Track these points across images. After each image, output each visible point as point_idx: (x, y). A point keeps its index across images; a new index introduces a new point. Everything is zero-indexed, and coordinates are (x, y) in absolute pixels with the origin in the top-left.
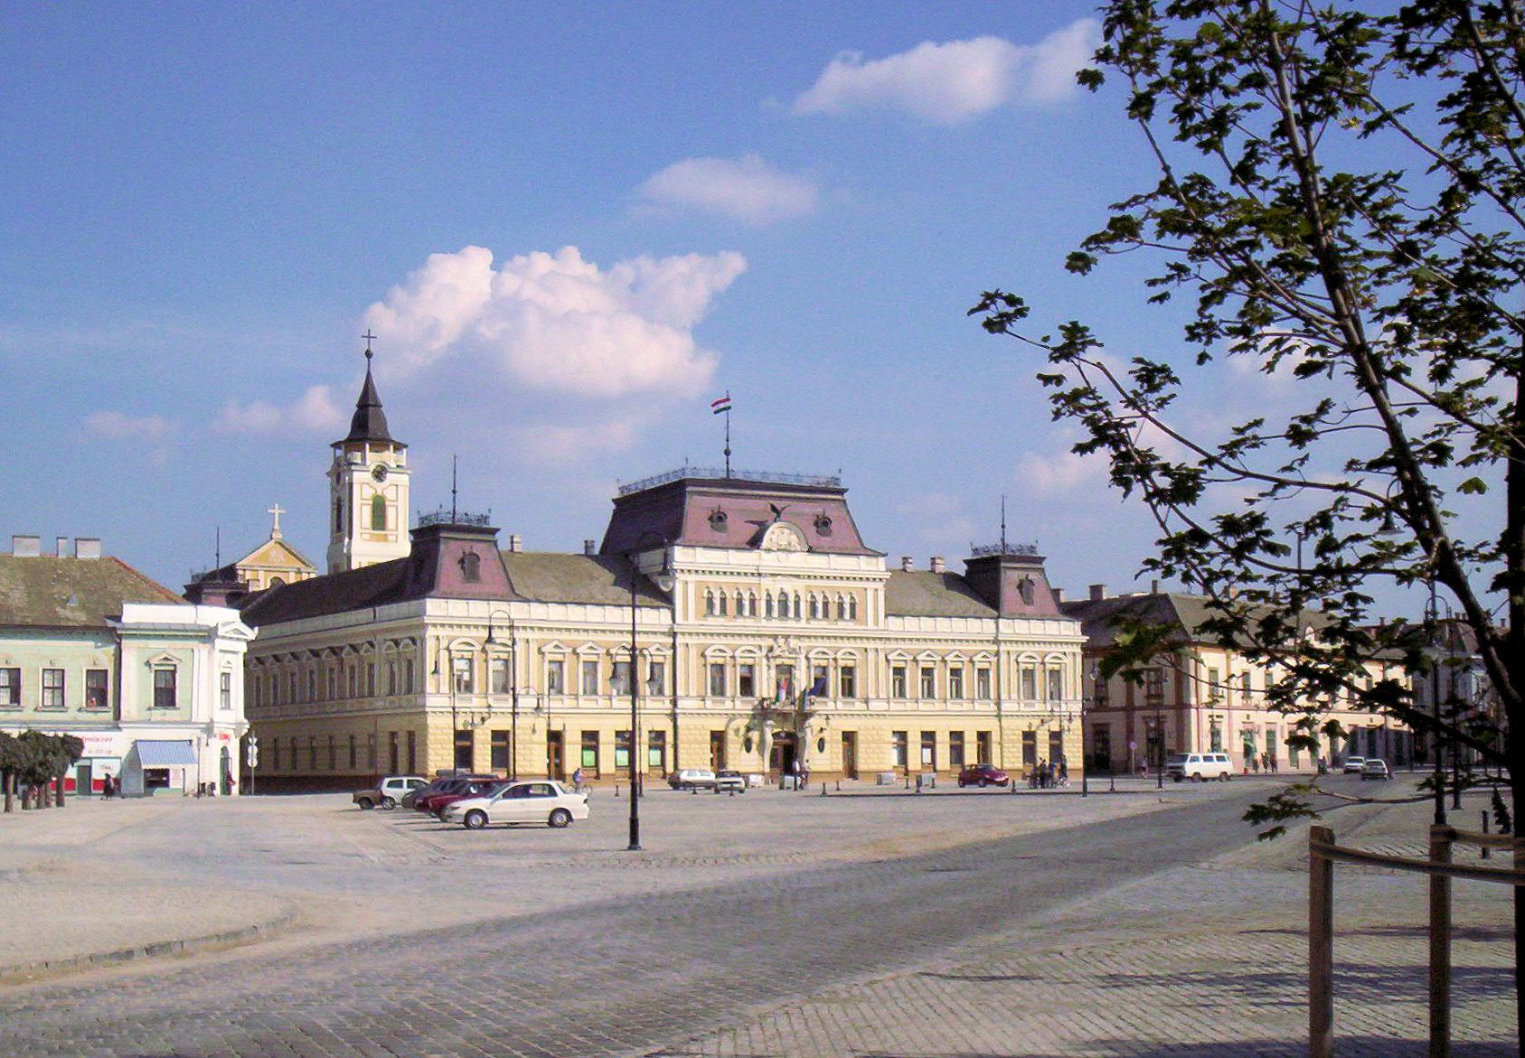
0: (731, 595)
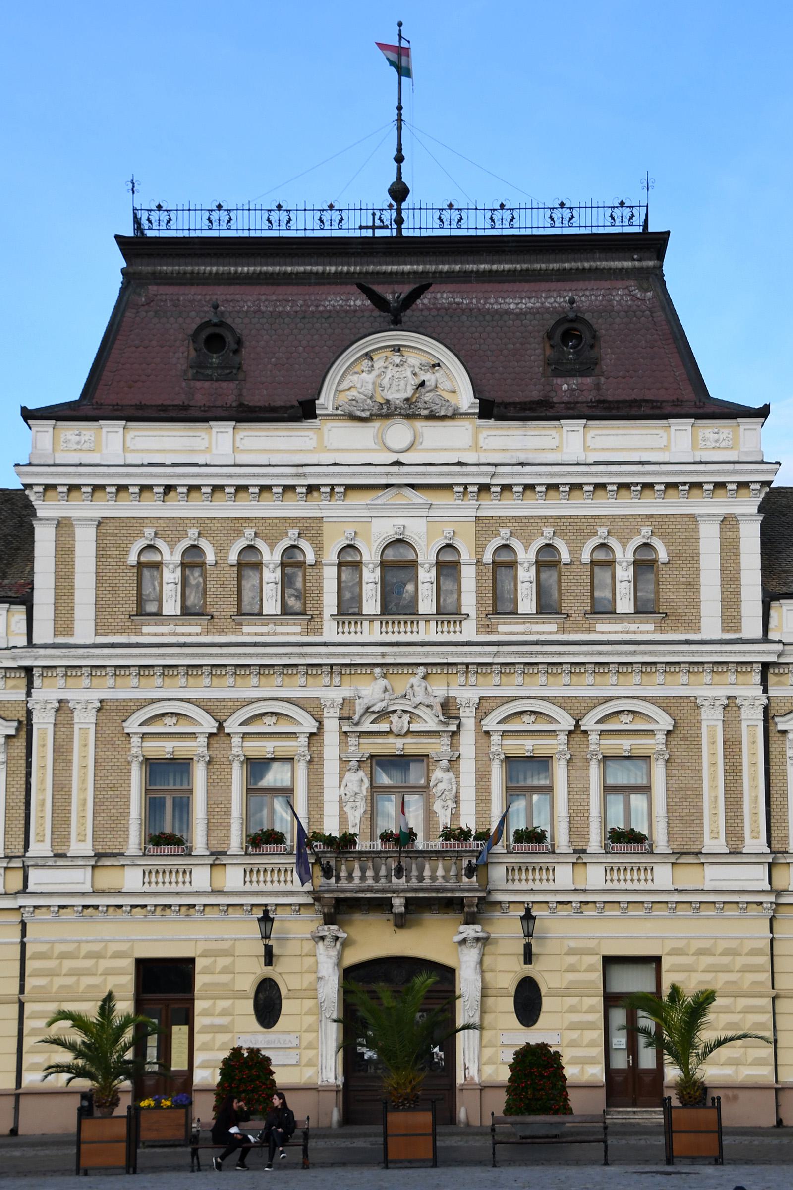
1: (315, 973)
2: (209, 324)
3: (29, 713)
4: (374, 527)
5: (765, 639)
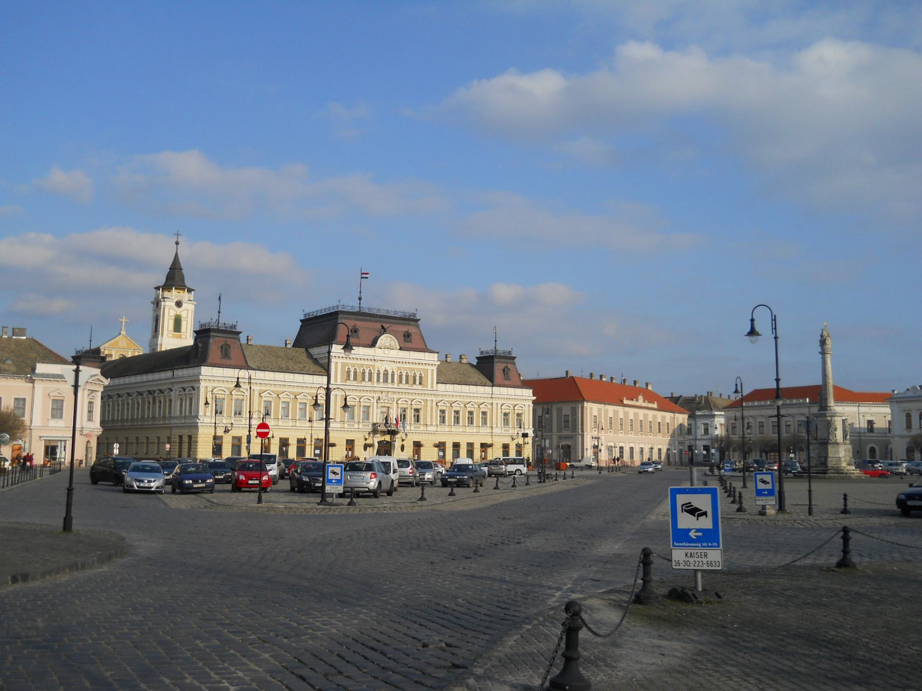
0: (360, 371)
4: (382, 367)
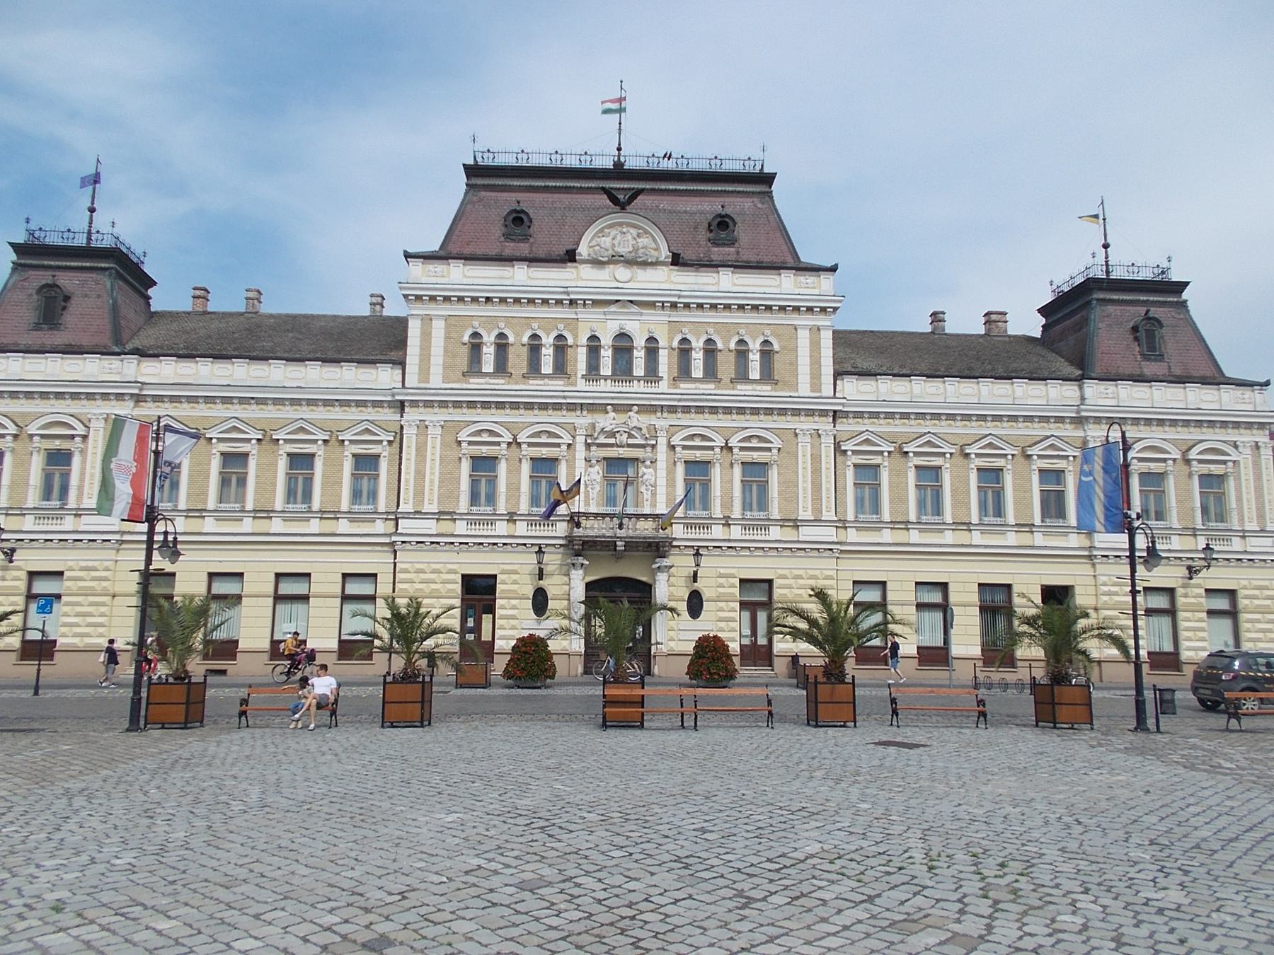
0: (518, 339)
1: (570, 587)
2: (515, 208)
3: (402, 427)
4: (608, 327)
5: (834, 397)
